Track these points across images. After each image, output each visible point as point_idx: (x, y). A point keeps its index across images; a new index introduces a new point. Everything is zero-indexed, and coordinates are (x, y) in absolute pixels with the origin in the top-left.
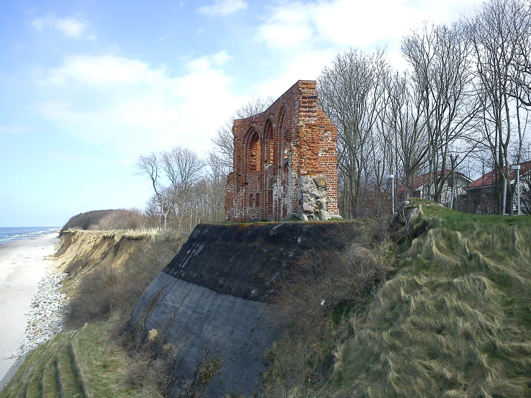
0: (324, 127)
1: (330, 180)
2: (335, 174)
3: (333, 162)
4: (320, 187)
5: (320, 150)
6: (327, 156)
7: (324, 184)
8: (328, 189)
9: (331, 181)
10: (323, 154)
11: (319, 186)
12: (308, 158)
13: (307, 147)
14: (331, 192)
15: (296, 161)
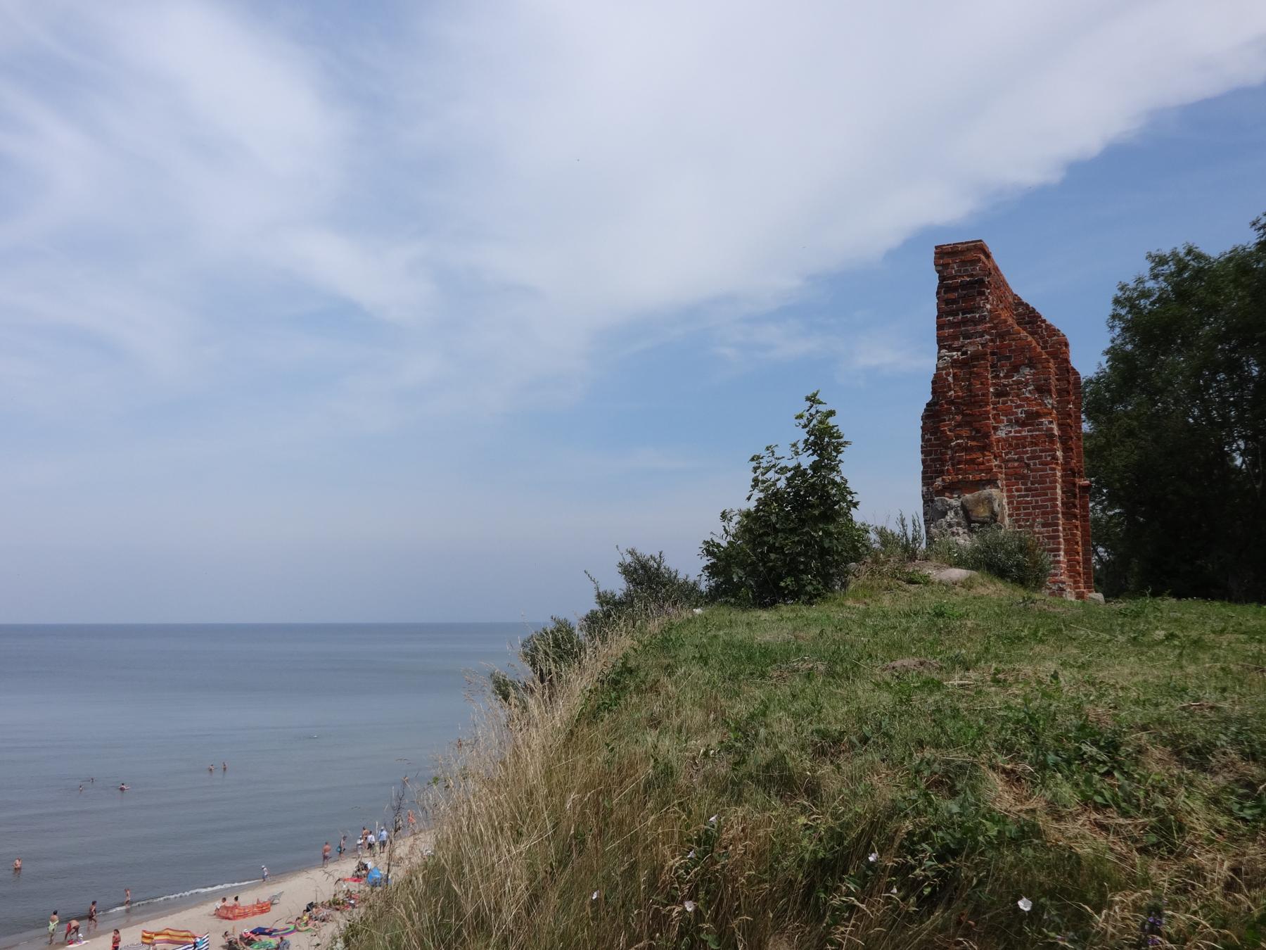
0: (1009, 358)
1: (1037, 501)
2: (1048, 484)
3: (1042, 451)
4: (974, 522)
5: (1002, 421)
6: (1023, 434)
7: (987, 514)
8: (1032, 526)
9: (1040, 503)
10: (1011, 432)
11: (973, 519)
12: (958, 445)
13: (959, 418)
14: (1041, 533)
15: (933, 456)
